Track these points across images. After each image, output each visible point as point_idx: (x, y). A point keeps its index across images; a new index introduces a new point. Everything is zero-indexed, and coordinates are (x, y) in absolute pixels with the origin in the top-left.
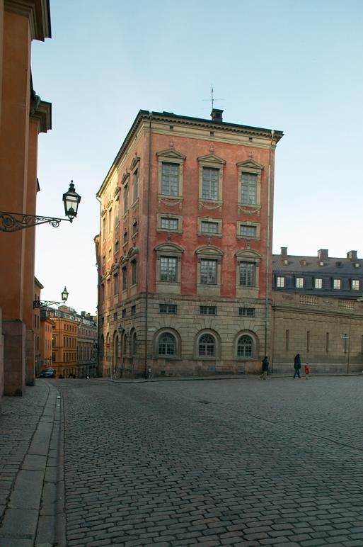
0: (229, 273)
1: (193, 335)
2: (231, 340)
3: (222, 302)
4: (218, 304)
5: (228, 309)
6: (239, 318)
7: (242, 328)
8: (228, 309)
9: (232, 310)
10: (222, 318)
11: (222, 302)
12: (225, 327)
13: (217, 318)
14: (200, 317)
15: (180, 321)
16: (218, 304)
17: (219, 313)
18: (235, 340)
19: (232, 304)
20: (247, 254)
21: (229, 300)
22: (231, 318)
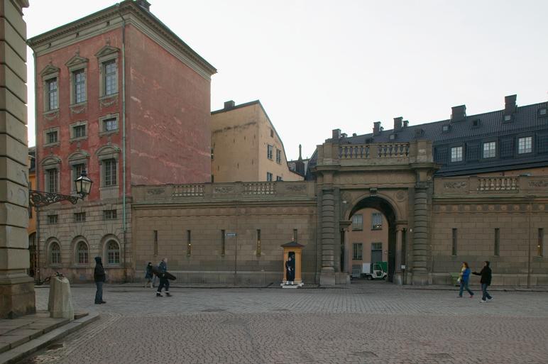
0: (95, 174)
1: (69, 243)
2: (97, 246)
3: (89, 207)
4: (87, 210)
5: (95, 214)
6: (103, 222)
7: (106, 233)
8: (95, 214)
9: (96, 213)
10: (90, 223)
11: (89, 207)
12: (92, 232)
13: (86, 224)
14: (74, 224)
15: (60, 230)
16: (87, 210)
17: (88, 219)
18: (101, 245)
19: (96, 208)
20: (106, 151)
21: (93, 204)
22: (95, 223)
